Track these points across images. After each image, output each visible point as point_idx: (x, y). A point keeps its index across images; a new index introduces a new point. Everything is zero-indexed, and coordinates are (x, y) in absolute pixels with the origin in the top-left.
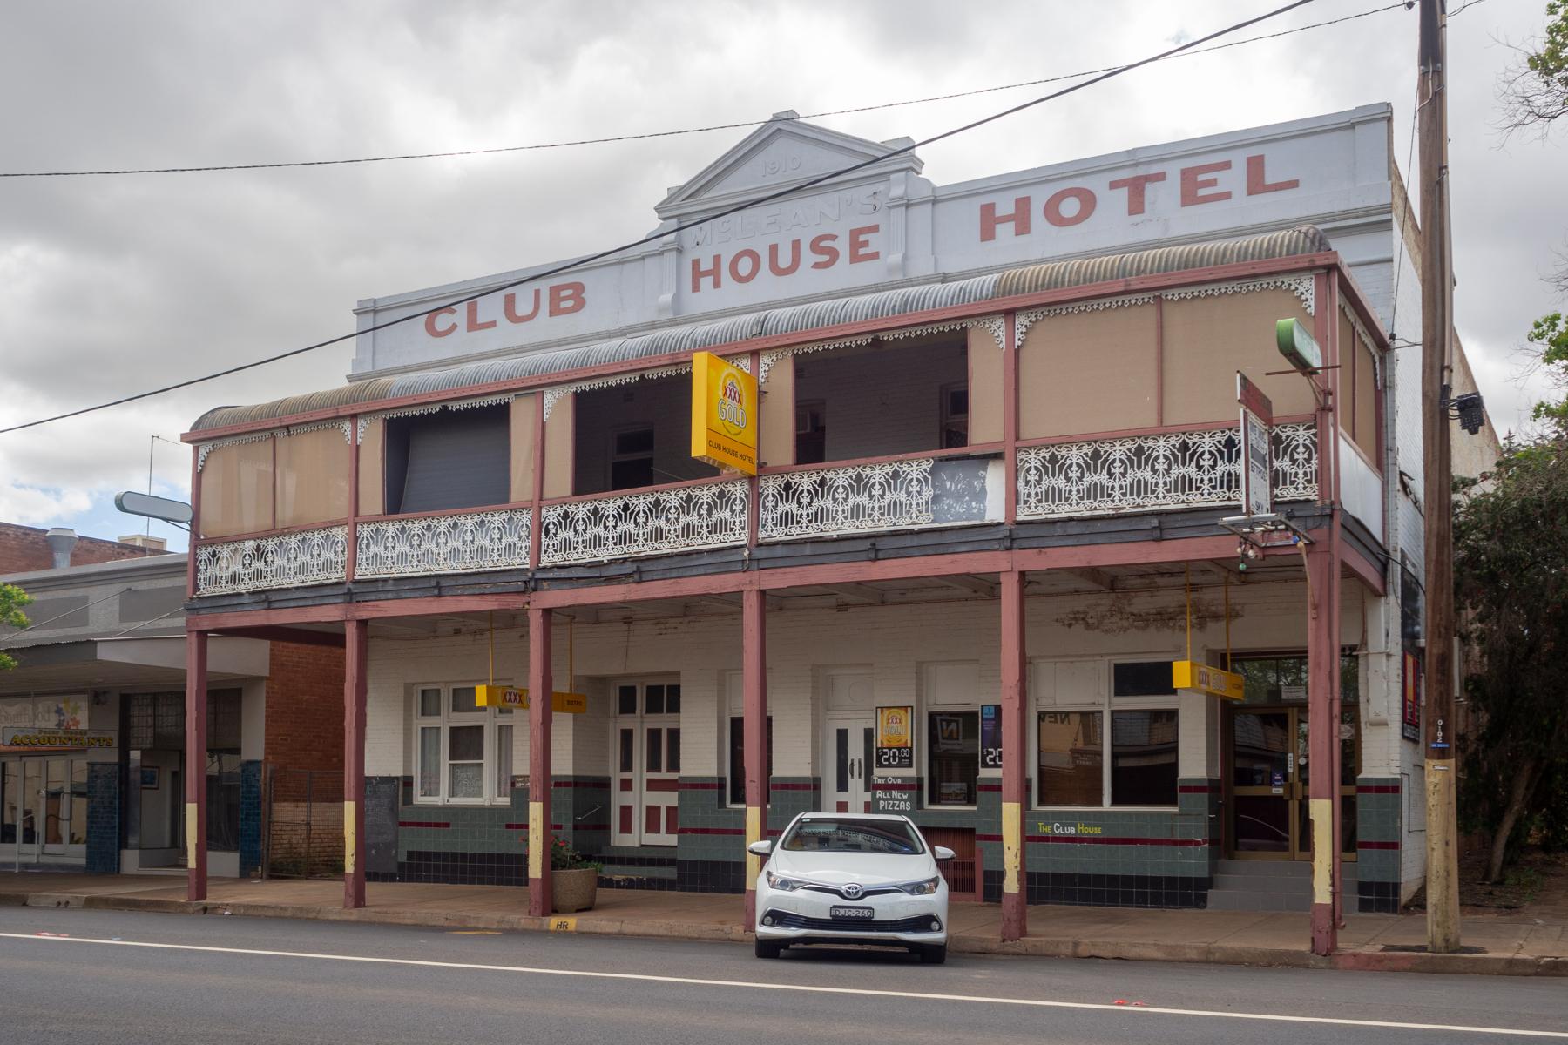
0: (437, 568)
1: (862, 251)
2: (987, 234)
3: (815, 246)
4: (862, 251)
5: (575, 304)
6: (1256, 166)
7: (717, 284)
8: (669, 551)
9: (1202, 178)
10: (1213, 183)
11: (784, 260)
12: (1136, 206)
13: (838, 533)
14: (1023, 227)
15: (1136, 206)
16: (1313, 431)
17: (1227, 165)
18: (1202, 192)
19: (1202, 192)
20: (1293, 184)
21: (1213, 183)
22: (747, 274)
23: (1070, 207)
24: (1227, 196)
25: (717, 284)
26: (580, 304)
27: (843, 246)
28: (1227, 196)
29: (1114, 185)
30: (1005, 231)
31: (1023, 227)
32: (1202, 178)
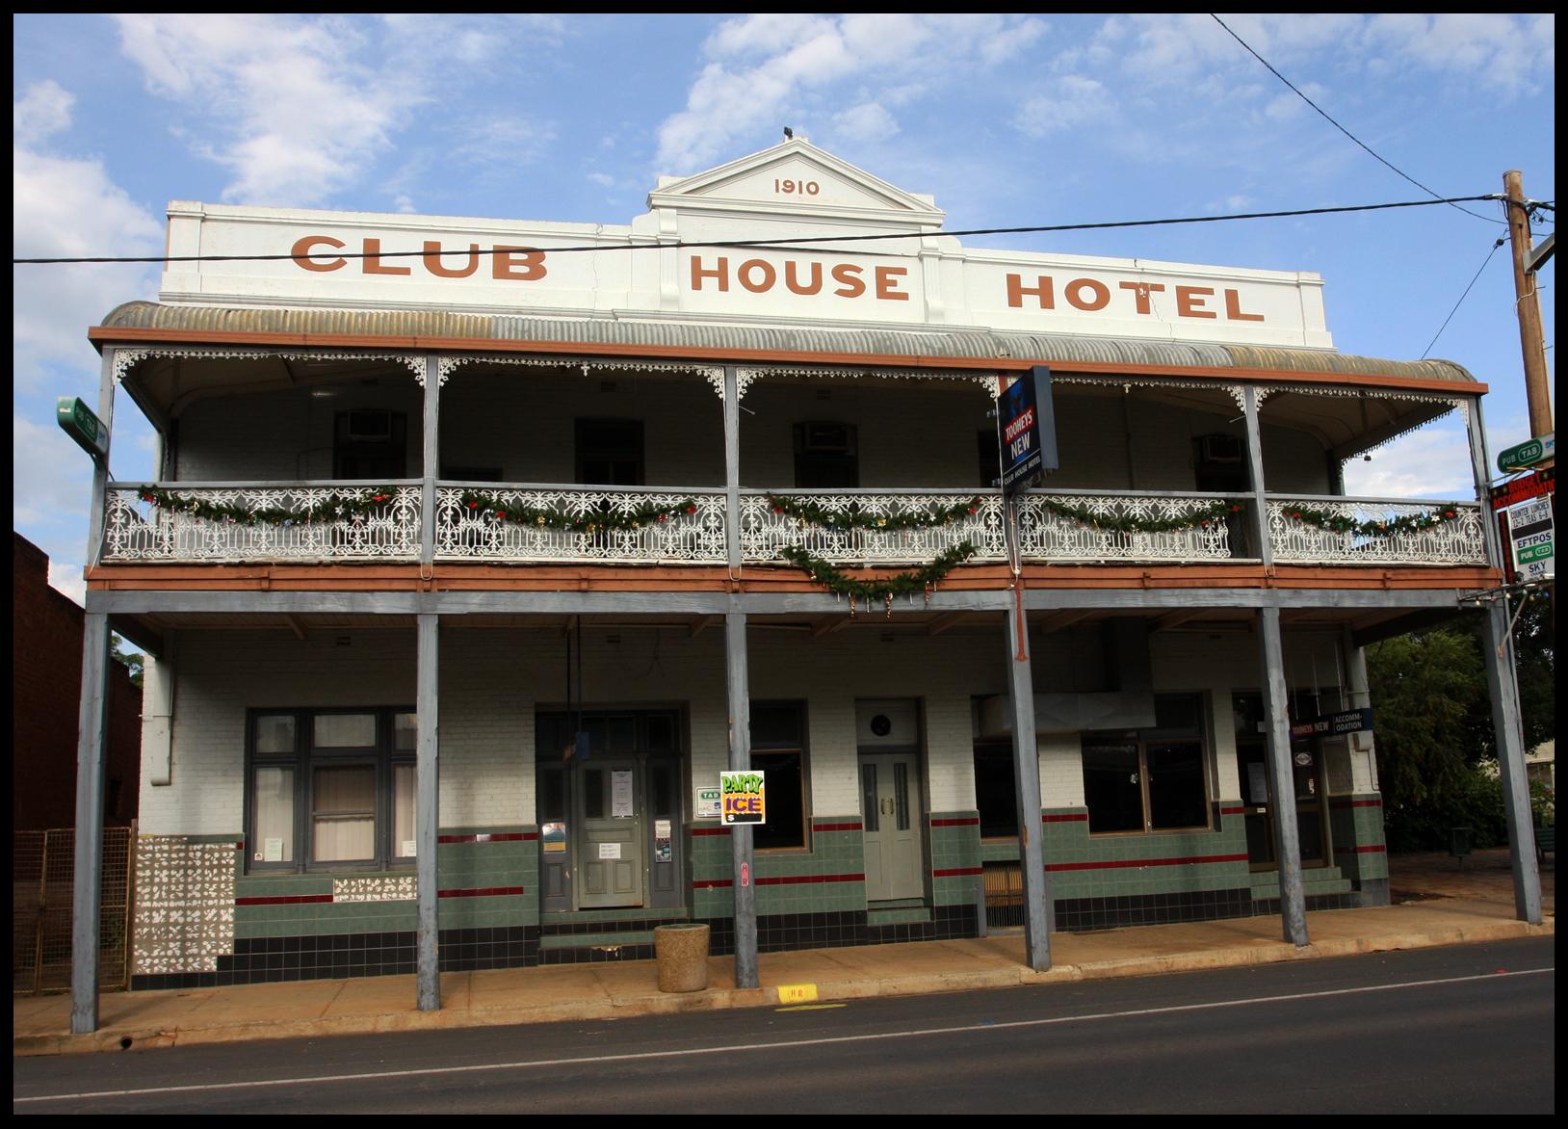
0: (208, 554)
1: (890, 289)
2: (1015, 300)
3: (838, 273)
4: (890, 289)
5: (528, 273)
6: (1232, 297)
7: (724, 286)
8: (487, 559)
9: (1192, 296)
10: (1201, 303)
11: (804, 279)
12: (1143, 306)
13: (1107, 559)
14: (1047, 302)
15: (1143, 306)
16: (1477, 514)
17: (1210, 292)
18: (1193, 308)
19: (1193, 308)
20: (1260, 318)
21: (1201, 303)
22: (763, 280)
23: (1088, 295)
24: (1212, 315)
25: (724, 286)
26: (537, 273)
27: (869, 278)
28: (1212, 315)
29: (1124, 285)
30: (1031, 302)
31: (1047, 302)
32: (1192, 296)
